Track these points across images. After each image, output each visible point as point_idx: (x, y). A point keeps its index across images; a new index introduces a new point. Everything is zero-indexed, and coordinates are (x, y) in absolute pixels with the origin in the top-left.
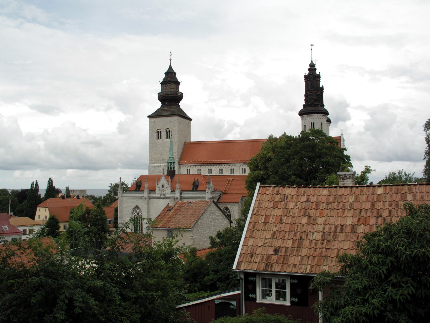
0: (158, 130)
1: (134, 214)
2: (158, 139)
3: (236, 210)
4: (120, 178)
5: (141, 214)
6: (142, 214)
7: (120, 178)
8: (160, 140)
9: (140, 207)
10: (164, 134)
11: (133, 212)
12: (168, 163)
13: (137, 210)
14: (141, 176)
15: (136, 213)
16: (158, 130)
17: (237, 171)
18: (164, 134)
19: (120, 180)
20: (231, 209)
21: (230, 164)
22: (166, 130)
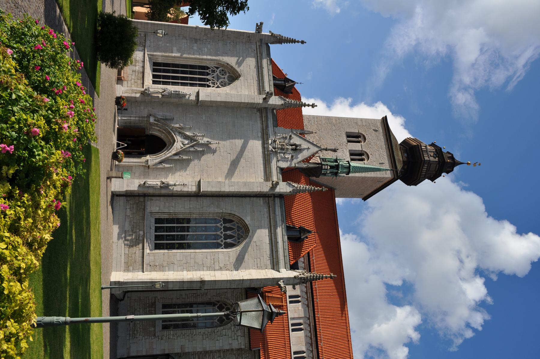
0: (362, 136)
1: (217, 68)
2: (348, 136)
3: (230, 342)
4: (303, 42)
5: (216, 86)
6: (218, 87)
7: (303, 42)
8: (345, 139)
9: (236, 83)
10: (357, 147)
11: (223, 66)
12: (336, 161)
13: (226, 77)
14: (299, 94)
15: (218, 72)
16: (362, 136)
17: (296, 312)
18: (357, 147)
19: (298, 42)
20: (231, 329)
21: (309, 295)
22: (365, 154)
